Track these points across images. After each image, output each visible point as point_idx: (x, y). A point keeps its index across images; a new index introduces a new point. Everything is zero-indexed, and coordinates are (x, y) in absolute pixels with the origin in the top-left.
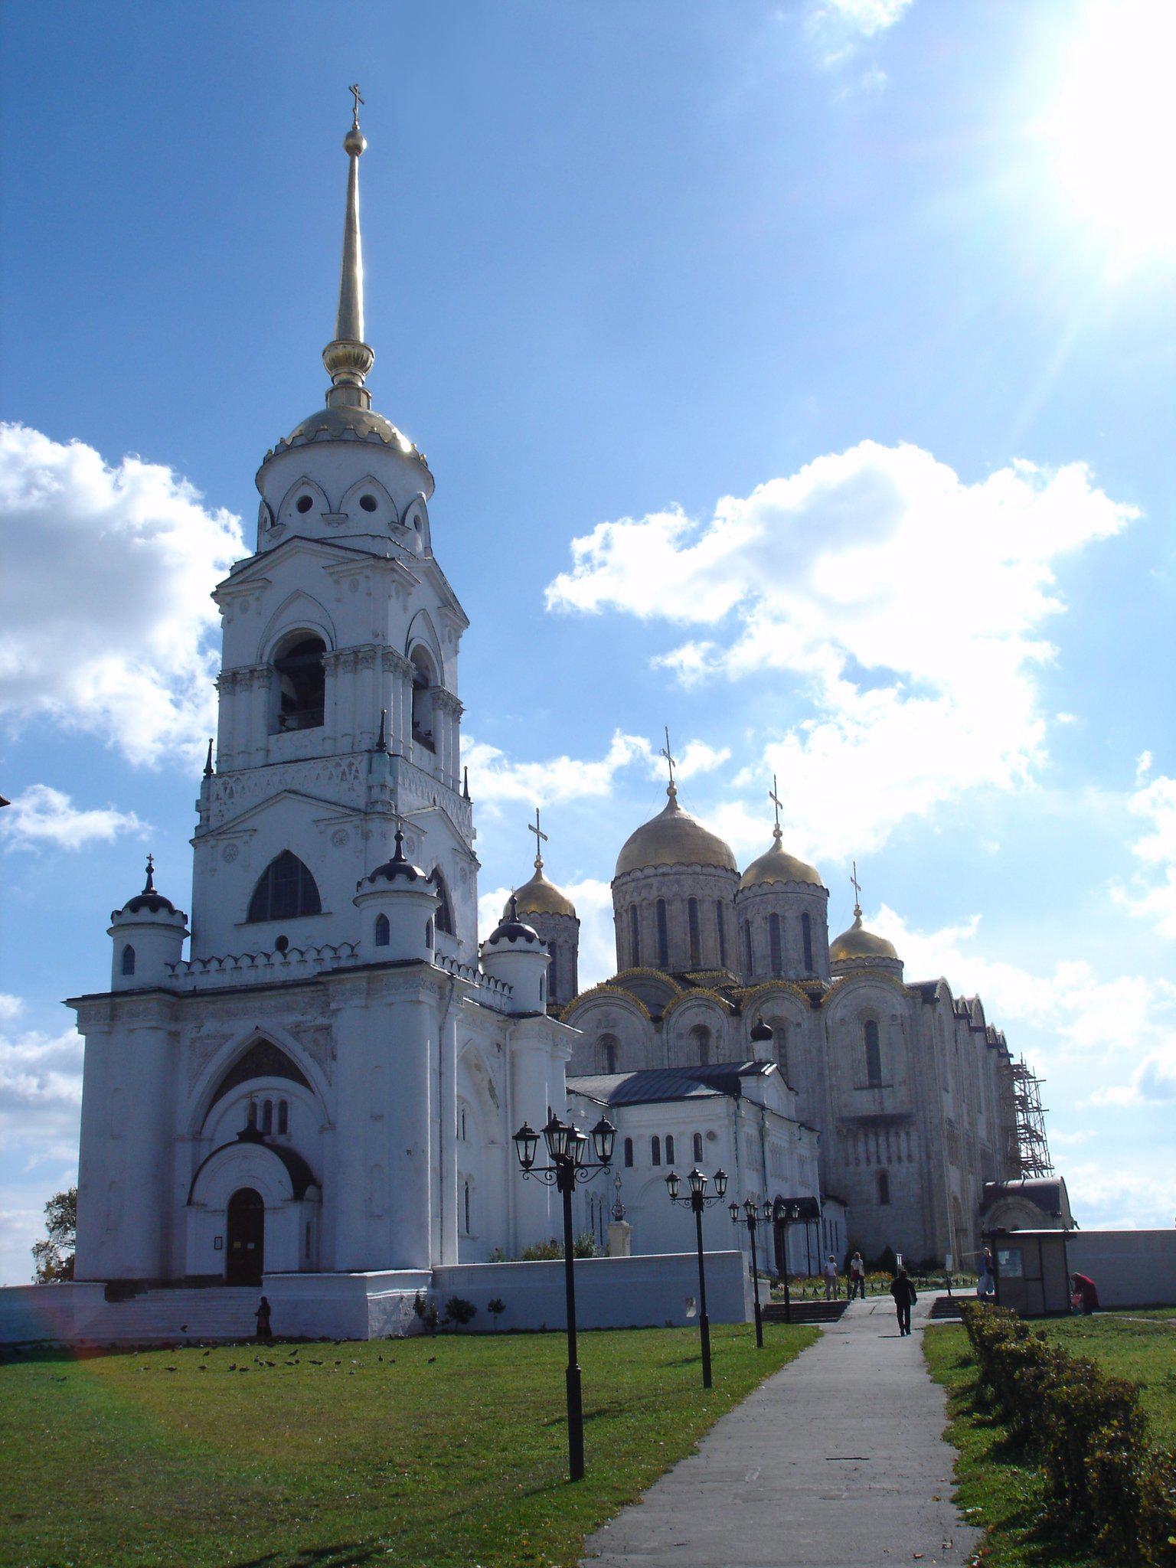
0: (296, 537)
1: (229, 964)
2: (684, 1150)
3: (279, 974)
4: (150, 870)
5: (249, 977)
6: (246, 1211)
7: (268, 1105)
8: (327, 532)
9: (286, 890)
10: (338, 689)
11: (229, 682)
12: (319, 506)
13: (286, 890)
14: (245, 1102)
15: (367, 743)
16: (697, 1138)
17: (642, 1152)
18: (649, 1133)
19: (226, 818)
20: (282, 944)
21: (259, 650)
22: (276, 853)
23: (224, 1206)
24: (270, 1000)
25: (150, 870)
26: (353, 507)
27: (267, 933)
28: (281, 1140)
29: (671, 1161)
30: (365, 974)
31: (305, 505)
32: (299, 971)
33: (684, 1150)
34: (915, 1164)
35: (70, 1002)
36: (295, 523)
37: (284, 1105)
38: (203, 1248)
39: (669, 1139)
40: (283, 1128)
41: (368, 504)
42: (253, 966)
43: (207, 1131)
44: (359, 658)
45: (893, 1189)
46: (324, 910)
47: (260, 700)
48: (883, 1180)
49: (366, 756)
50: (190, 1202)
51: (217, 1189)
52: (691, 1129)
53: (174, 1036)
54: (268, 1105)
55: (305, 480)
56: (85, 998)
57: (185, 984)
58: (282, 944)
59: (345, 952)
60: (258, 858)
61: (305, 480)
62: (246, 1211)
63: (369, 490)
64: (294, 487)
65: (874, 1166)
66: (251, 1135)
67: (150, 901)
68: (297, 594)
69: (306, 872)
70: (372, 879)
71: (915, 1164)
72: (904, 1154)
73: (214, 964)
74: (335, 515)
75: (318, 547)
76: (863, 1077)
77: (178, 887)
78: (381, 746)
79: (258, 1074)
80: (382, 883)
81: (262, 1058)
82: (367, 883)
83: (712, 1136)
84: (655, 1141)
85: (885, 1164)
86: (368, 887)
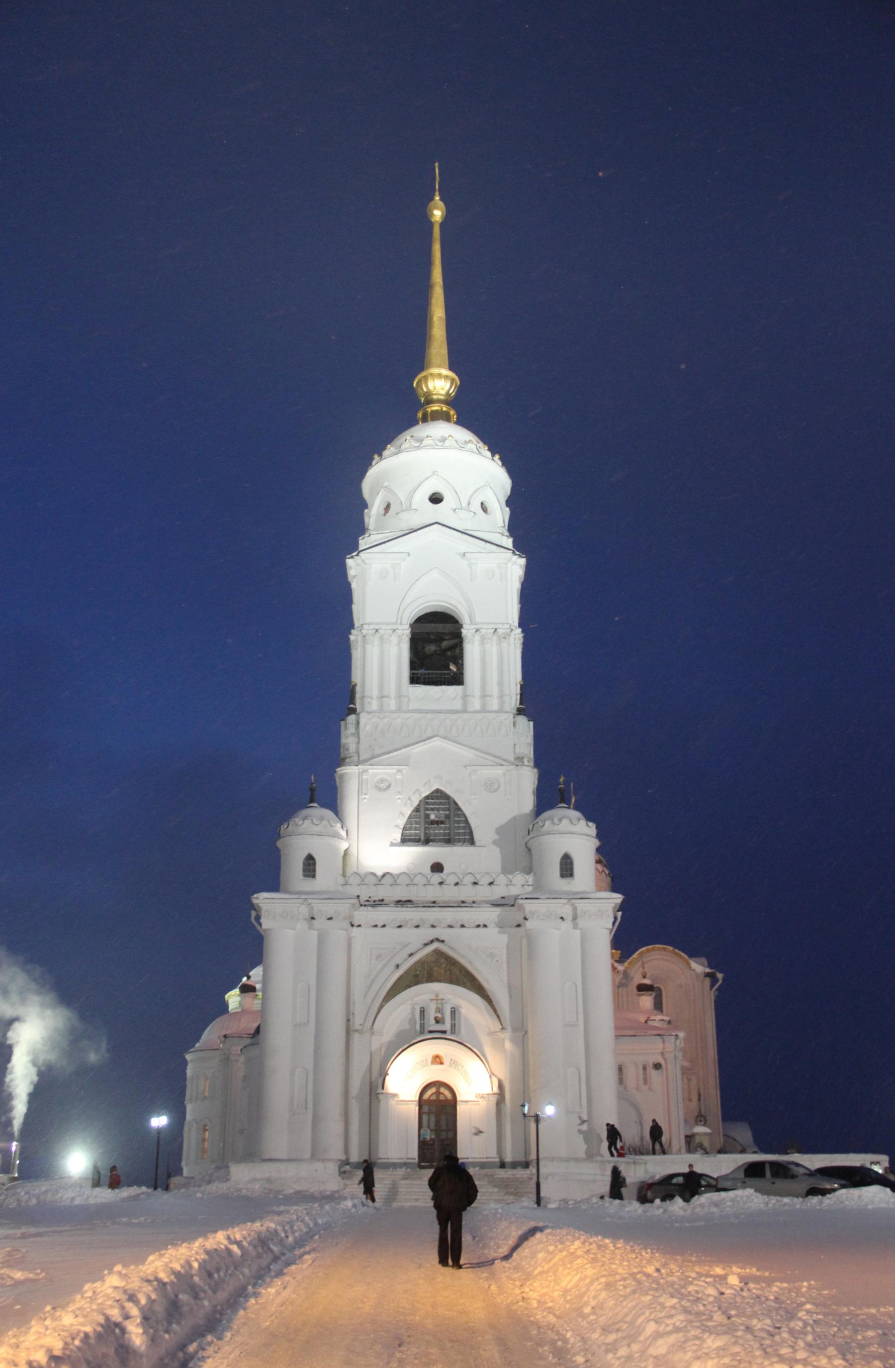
0: (437, 523)
19: (378, 751)
31: (436, 499)
37: (454, 1012)
46: (477, 844)
79: (431, 979)
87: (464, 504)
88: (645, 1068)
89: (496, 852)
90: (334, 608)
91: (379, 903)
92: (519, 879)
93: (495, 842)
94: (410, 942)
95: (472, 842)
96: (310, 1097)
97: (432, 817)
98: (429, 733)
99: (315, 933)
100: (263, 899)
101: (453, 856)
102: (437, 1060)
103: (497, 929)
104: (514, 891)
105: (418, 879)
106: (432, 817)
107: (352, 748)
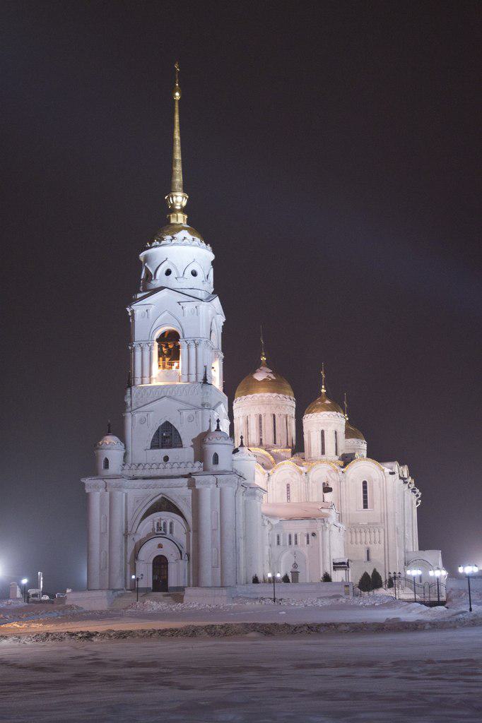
2: (302, 540)
3: (168, 472)
5: (159, 473)
6: (160, 564)
8: (176, 285)
12: (174, 274)
15: (201, 377)
19: (140, 404)
20: (166, 459)
22: (163, 422)
23: (151, 561)
24: (166, 482)
33: (302, 540)
34: (382, 546)
37: (171, 524)
39: (296, 536)
40: (171, 532)
41: (194, 274)
45: (372, 556)
49: (200, 385)
51: (149, 552)
58: (166, 459)
62: (160, 564)
69: (176, 430)
72: (377, 540)
73: (141, 467)
83: (314, 534)
84: (290, 536)
85: (369, 545)
87: (181, 276)
88: (308, 537)
89: (192, 450)
90: (125, 327)
91: (136, 479)
92: (198, 464)
93: (192, 446)
96: (108, 564)
97: (164, 434)
98: (162, 395)
99: (108, 493)
100: (87, 481)
103: (187, 488)
104: (195, 470)
106: (164, 434)
107: (129, 403)
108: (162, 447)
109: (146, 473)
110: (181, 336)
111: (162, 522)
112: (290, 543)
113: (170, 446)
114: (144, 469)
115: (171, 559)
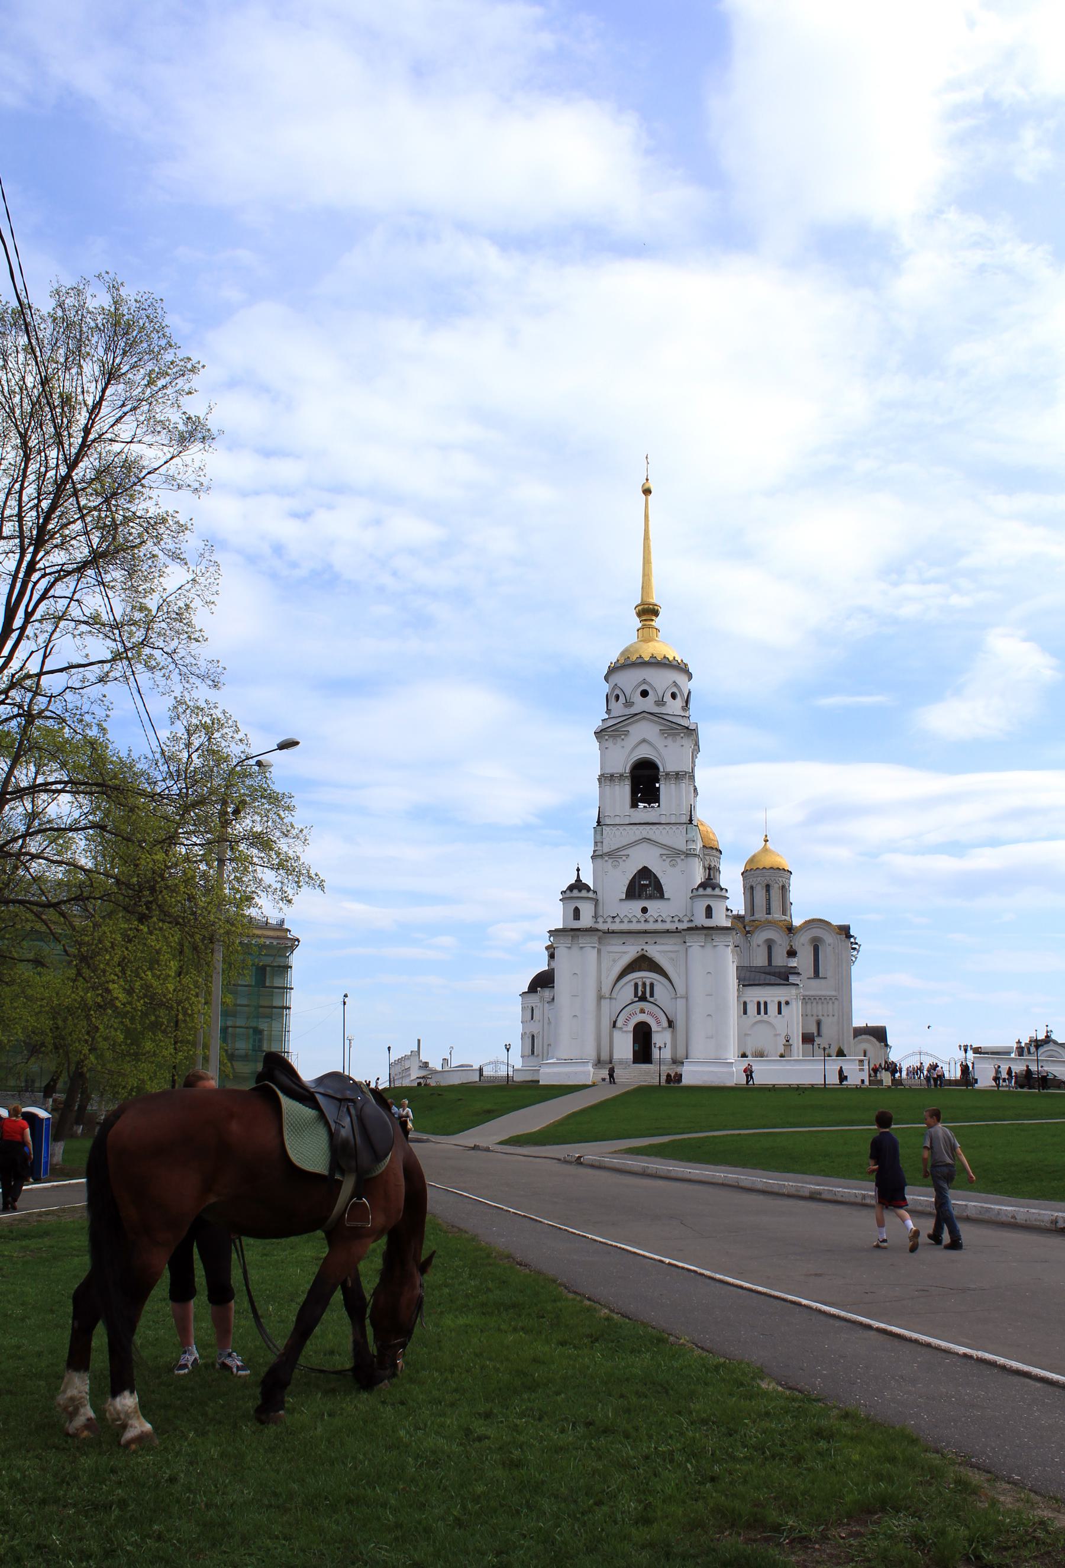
1: (626, 920)
2: (773, 1009)
4: (578, 870)
7: (644, 984)
9: (644, 886)
10: (665, 789)
11: (606, 779)
13: (644, 886)
14: (633, 983)
16: (780, 1003)
17: (752, 1009)
18: (756, 1000)
20: (644, 910)
21: (622, 763)
25: (578, 870)
26: (668, 698)
27: (636, 906)
28: (651, 999)
29: (766, 1013)
30: (705, 932)
31: (645, 694)
32: (659, 926)
33: (773, 1009)
34: (836, 1017)
35: (550, 932)
36: (641, 705)
37: (652, 985)
38: (624, 1047)
39: (766, 1003)
40: (652, 995)
41: (674, 696)
42: (638, 922)
43: (614, 995)
44: (678, 776)
47: (624, 790)
48: (819, 1023)
50: (614, 1026)
52: (776, 1000)
53: (599, 951)
54: (644, 984)
55: (644, 682)
56: (557, 930)
57: (601, 926)
58: (644, 910)
59: (686, 919)
60: (631, 869)
61: (644, 682)
63: (675, 690)
64: (639, 685)
65: (815, 1018)
66: (643, 999)
67: (578, 885)
68: (644, 741)
70: (697, 889)
71: (836, 1017)
73: (617, 920)
74: (661, 703)
75: (656, 719)
76: (812, 973)
77: (588, 879)
78: (691, 820)
80: (709, 891)
81: (643, 963)
82: (701, 890)
83: (787, 1003)
84: (759, 1003)
85: (820, 1017)
86: (701, 891)
94: (630, 951)
95: (662, 896)
101: (653, 906)
102: (642, 1011)
105: (634, 920)
108: (639, 897)
109: (625, 927)
110: (661, 769)
111: (640, 984)
112: (759, 1013)
113: (650, 897)
114: (622, 922)
115: (654, 1027)
